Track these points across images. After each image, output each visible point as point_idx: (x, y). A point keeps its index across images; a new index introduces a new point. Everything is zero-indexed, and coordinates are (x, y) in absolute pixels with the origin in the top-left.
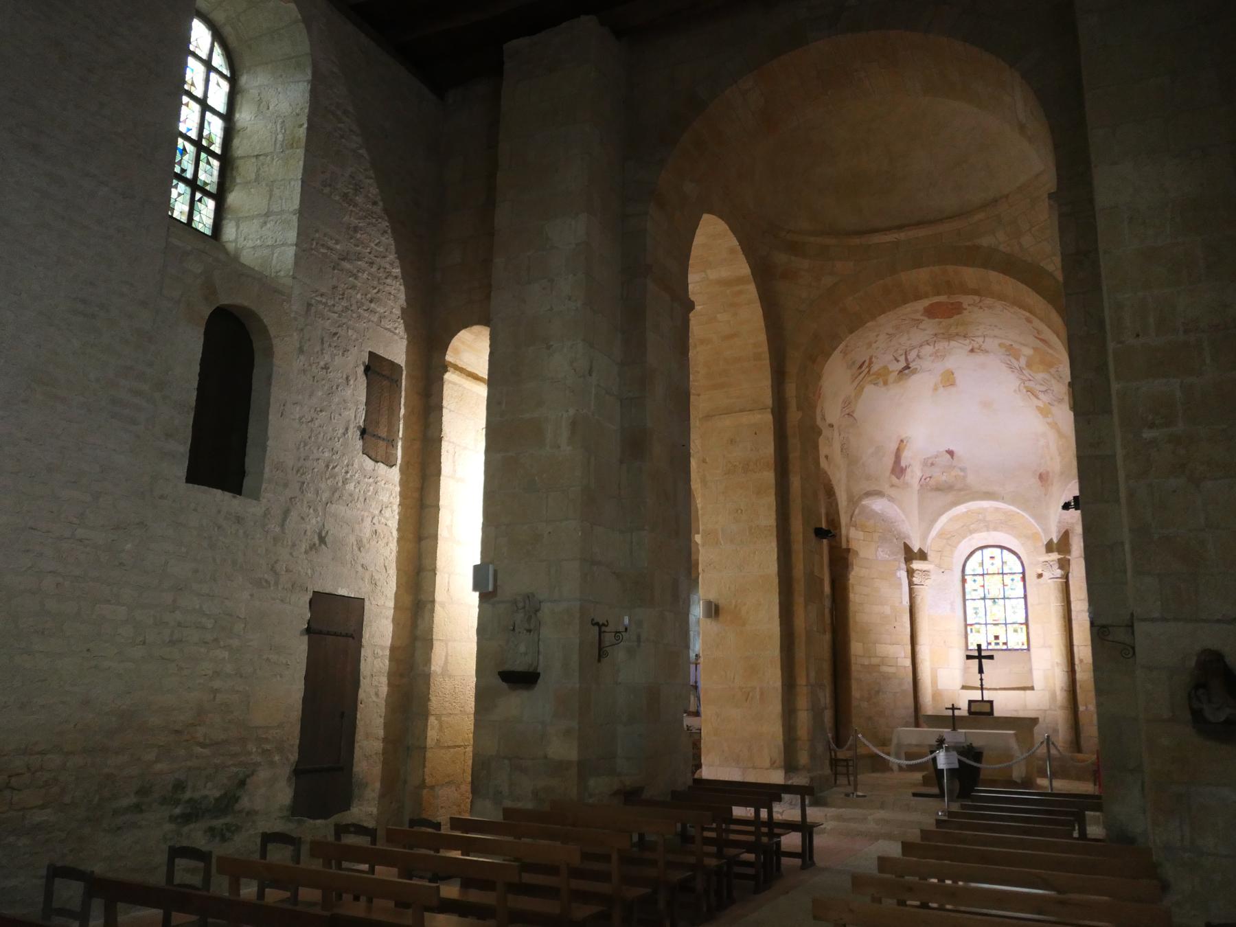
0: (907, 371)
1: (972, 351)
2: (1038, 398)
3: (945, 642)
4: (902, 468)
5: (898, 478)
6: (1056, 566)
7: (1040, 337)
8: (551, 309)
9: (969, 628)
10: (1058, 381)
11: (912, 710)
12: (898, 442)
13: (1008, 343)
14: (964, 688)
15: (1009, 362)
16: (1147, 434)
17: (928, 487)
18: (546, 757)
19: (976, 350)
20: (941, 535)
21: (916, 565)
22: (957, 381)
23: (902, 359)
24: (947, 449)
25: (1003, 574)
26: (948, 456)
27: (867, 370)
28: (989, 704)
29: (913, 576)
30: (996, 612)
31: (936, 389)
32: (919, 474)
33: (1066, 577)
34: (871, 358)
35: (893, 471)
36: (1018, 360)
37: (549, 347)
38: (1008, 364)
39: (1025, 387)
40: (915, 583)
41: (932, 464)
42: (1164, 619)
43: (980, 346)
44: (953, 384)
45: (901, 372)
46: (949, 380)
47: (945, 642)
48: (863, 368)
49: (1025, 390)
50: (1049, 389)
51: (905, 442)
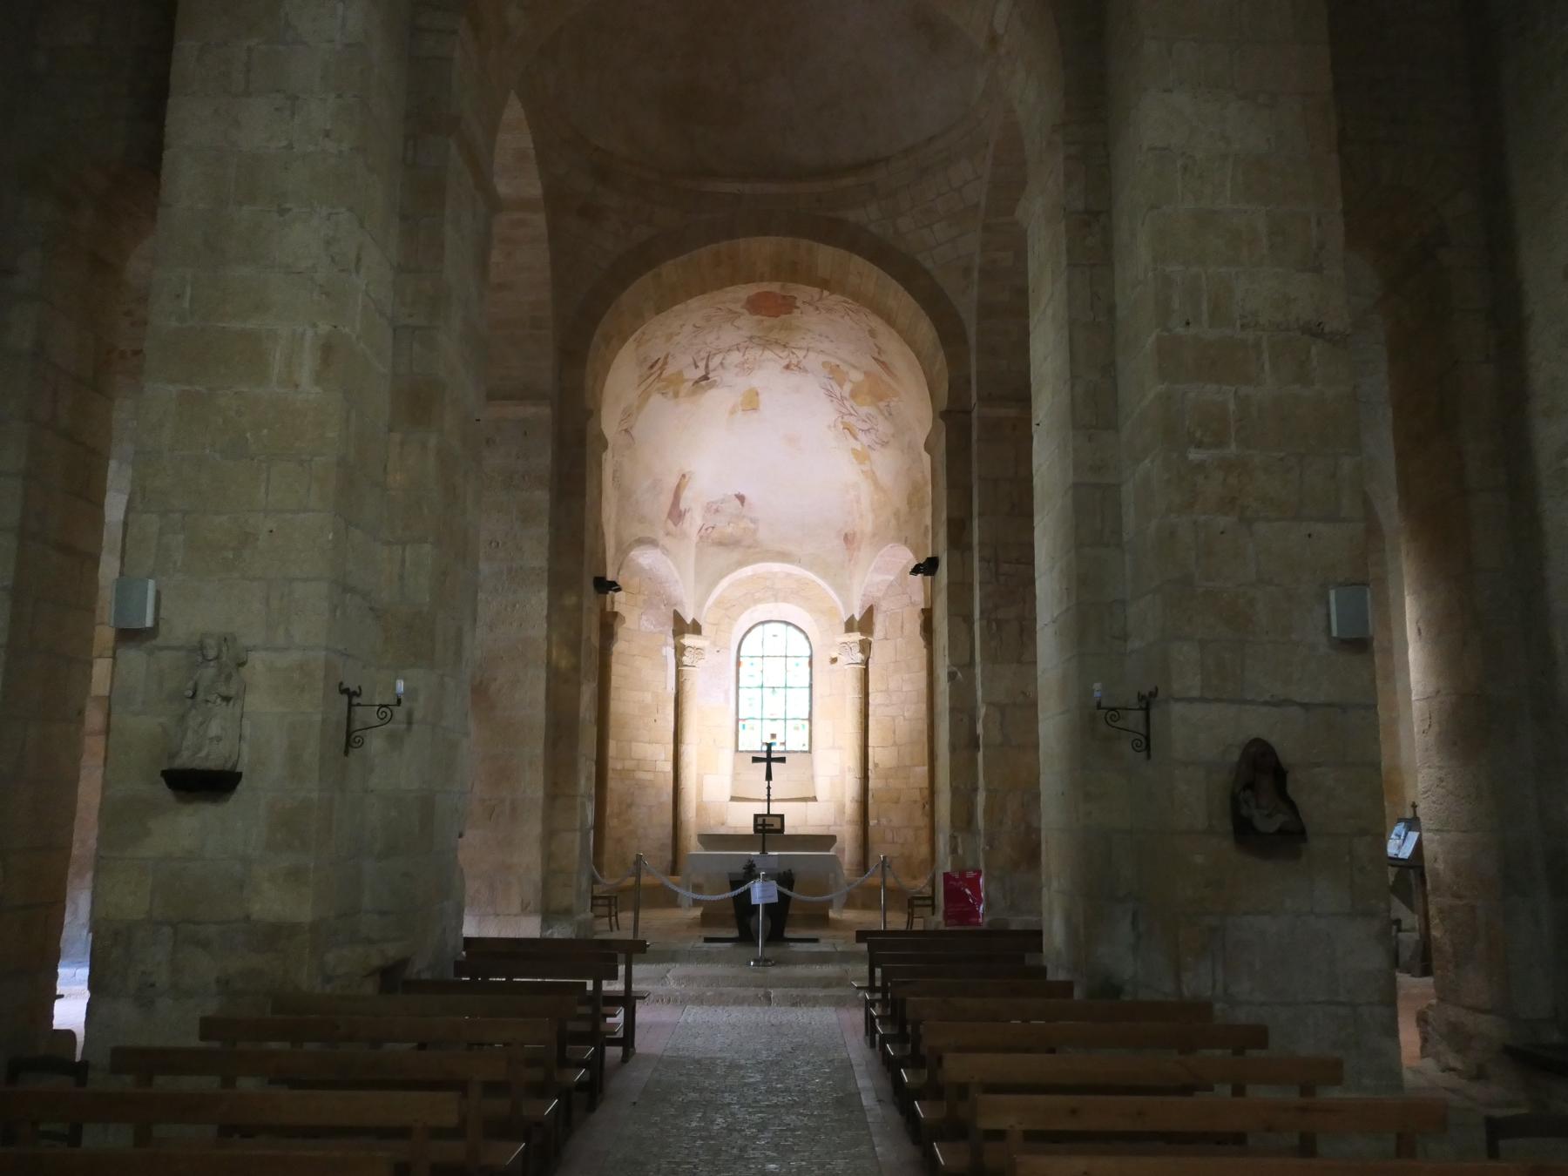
0: (703, 383)
1: (787, 367)
2: (856, 438)
3: (714, 741)
4: (681, 511)
5: (676, 525)
6: (857, 648)
7: (881, 359)
8: (290, 147)
9: (741, 723)
10: (886, 418)
11: (669, 829)
12: (680, 477)
13: (834, 361)
14: (733, 799)
15: (829, 388)
16: (1194, 455)
18: (247, 918)
19: (792, 367)
20: (718, 603)
21: (689, 640)
22: (761, 407)
23: (702, 365)
24: (737, 493)
25: (786, 657)
26: (738, 502)
27: (659, 372)
28: (779, 819)
29: (682, 654)
30: (774, 705)
31: (733, 412)
32: (699, 522)
33: (866, 663)
34: (666, 358)
35: (670, 515)
36: (841, 385)
37: (282, 212)
38: (828, 390)
39: (842, 423)
40: (685, 663)
41: (717, 511)
42: (1202, 700)
43: (799, 362)
44: (755, 409)
45: (697, 382)
46: (751, 402)
47: (714, 741)
48: (655, 369)
49: (842, 427)
50: (873, 428)
51: (687, 477)
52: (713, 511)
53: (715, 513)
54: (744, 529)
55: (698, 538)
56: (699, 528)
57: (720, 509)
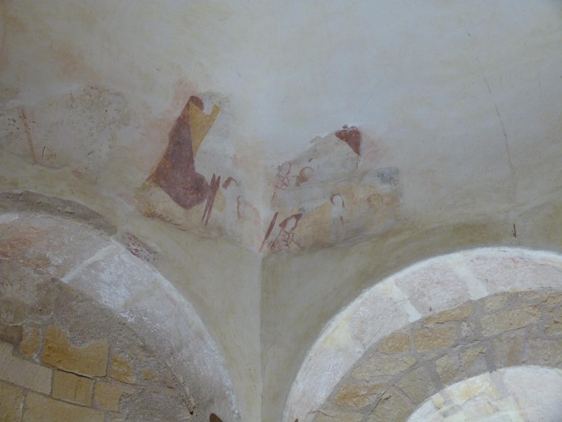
17: (293, 246)
26: (345, 148)
41: (302, 179)
52: (293, 182)
53: (298, 185)
54: (369, 200)
55: (266, 248)
56: (264, 227)
57: (307, 172)
